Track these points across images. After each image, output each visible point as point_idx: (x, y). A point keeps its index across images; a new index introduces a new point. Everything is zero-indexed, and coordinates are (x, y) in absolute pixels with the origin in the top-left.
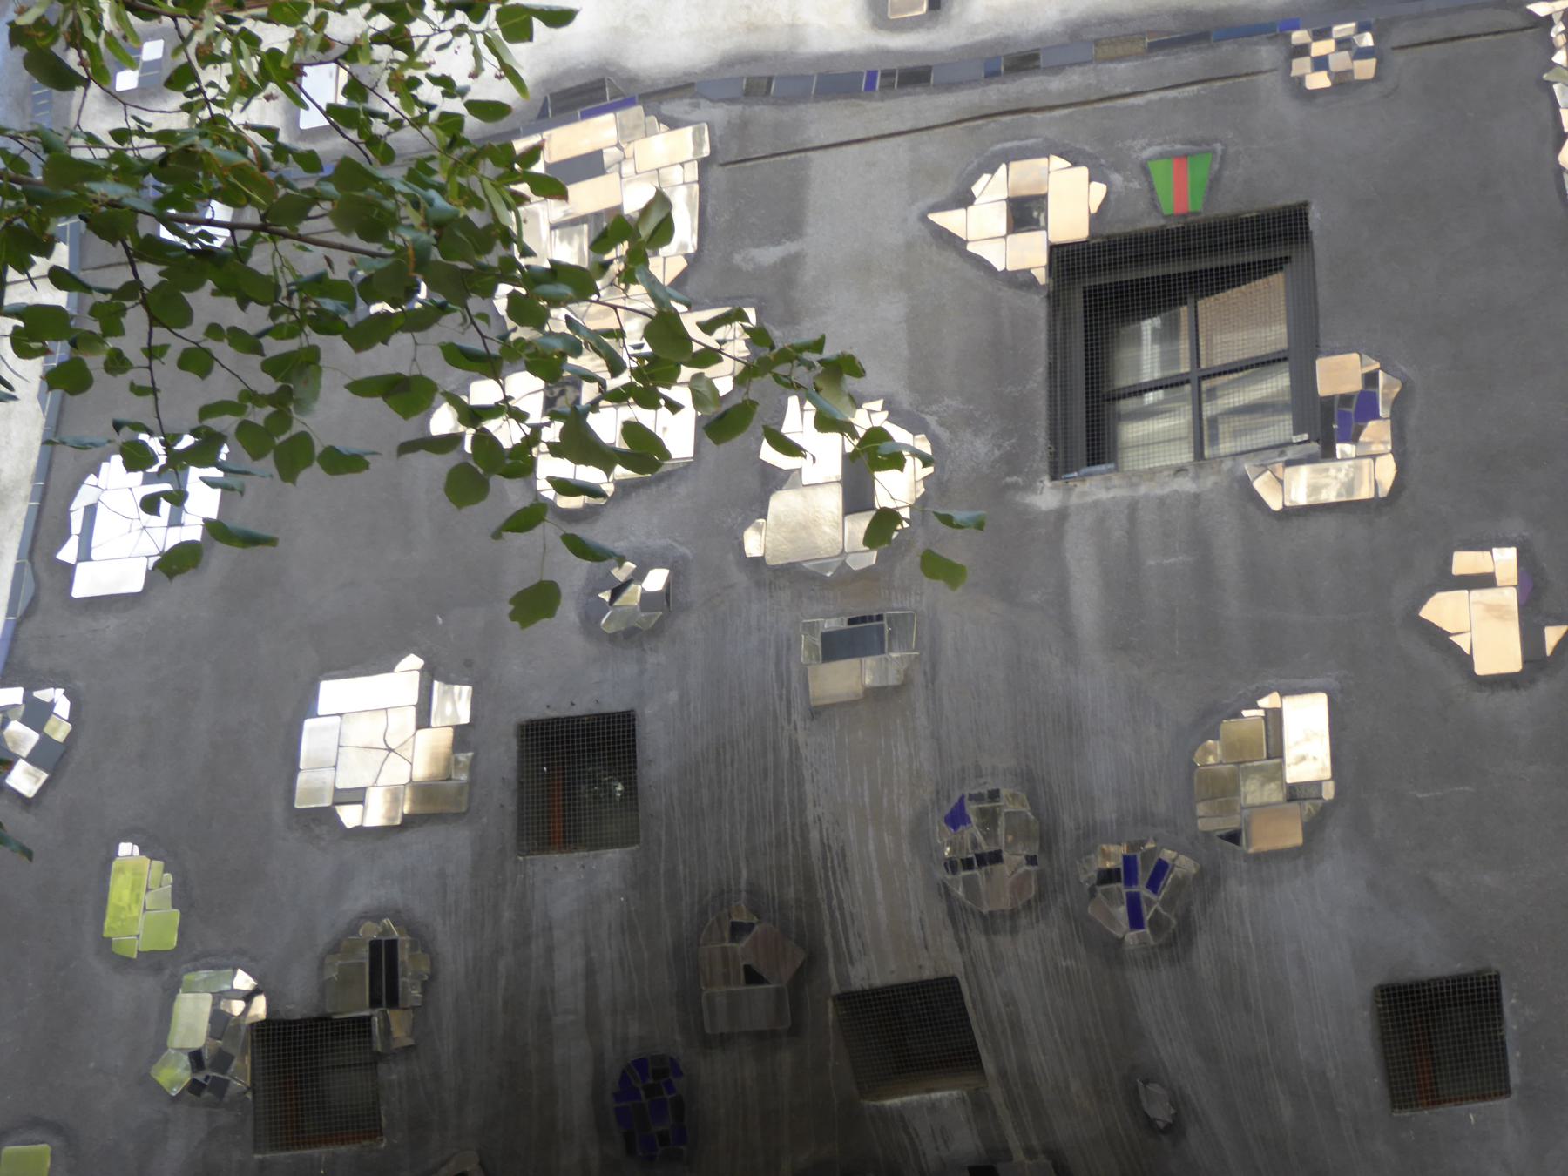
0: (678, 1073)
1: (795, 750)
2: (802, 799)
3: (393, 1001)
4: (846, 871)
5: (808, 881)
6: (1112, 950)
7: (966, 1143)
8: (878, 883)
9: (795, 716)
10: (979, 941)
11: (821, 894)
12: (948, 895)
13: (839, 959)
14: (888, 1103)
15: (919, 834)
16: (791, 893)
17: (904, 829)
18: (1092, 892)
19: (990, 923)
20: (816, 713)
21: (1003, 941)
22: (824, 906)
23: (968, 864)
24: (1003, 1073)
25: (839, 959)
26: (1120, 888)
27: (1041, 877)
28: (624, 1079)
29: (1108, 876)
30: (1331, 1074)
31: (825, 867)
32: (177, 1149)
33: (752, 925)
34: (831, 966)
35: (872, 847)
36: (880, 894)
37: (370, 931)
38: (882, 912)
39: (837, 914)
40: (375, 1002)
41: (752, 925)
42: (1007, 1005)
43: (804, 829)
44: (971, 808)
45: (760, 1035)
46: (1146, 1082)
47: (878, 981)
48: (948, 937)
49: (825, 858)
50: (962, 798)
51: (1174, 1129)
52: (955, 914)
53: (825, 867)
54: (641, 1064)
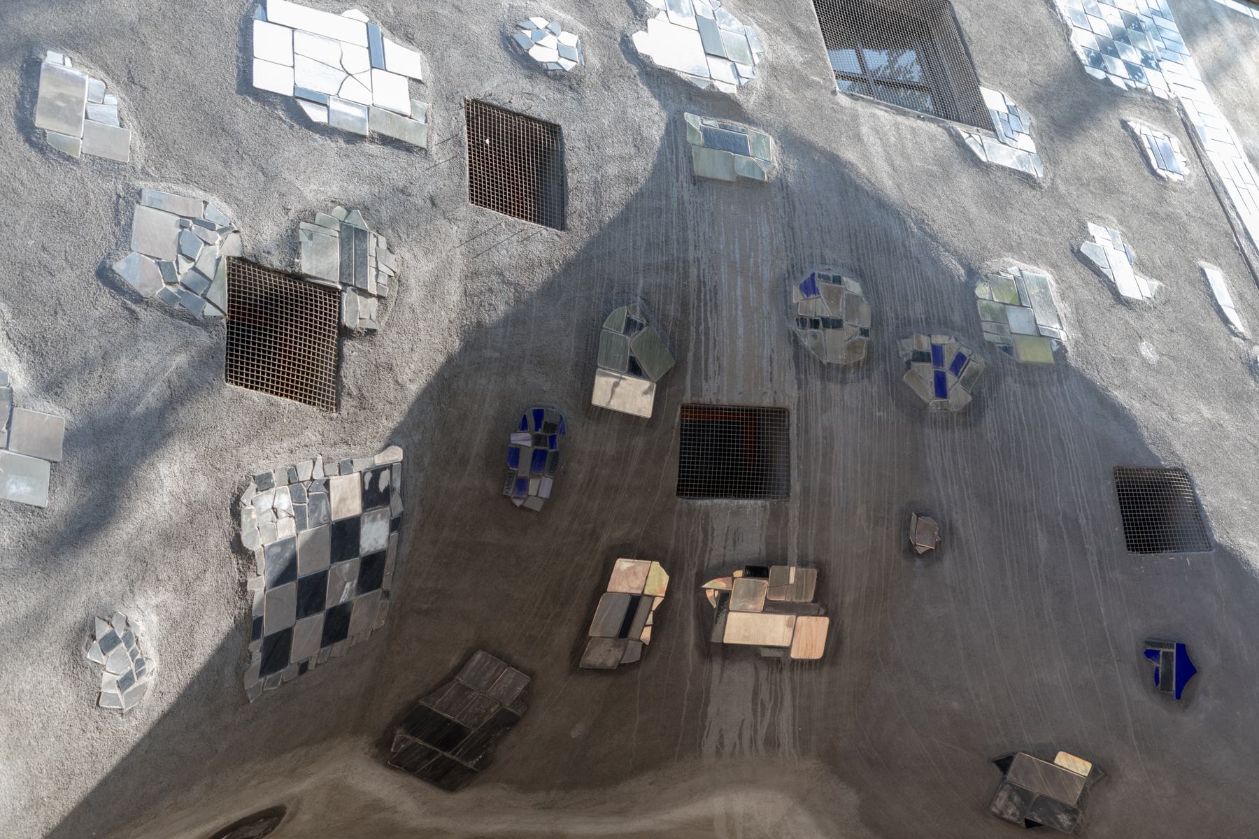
0: (563, 432)
1: (681, 202)
2: (685, 240)
4: (716, 306)
6: (917, 411)
8: (741, 321)
9: (681, 177)
10: (815, 384)
11: (692, 318)
12: (796, 342)
13: (696, 372)
15: (780, 293)
17: (766, 285)
18: (908, 364)
19: (826, 371)
21: (834, 388)
22: (693, 329)
23: (815, 324)
24: (806, 491)
25: (696, 372)
27: (869, 346)
29: (921, 357)
30: (1083, 521)
31: (699, 300)
33: (641, 326)
34: (688, 377)
35: (739, 293)
36: (741, 330)
38: (740, 344)
39: (703, 338)
42: (825, 438)
44: (820, 284)
47: (725, 400)
48: (790, 375)
49: (699, 291)
50: (813, 275)
52: (800, 358)
53: (699, 300)
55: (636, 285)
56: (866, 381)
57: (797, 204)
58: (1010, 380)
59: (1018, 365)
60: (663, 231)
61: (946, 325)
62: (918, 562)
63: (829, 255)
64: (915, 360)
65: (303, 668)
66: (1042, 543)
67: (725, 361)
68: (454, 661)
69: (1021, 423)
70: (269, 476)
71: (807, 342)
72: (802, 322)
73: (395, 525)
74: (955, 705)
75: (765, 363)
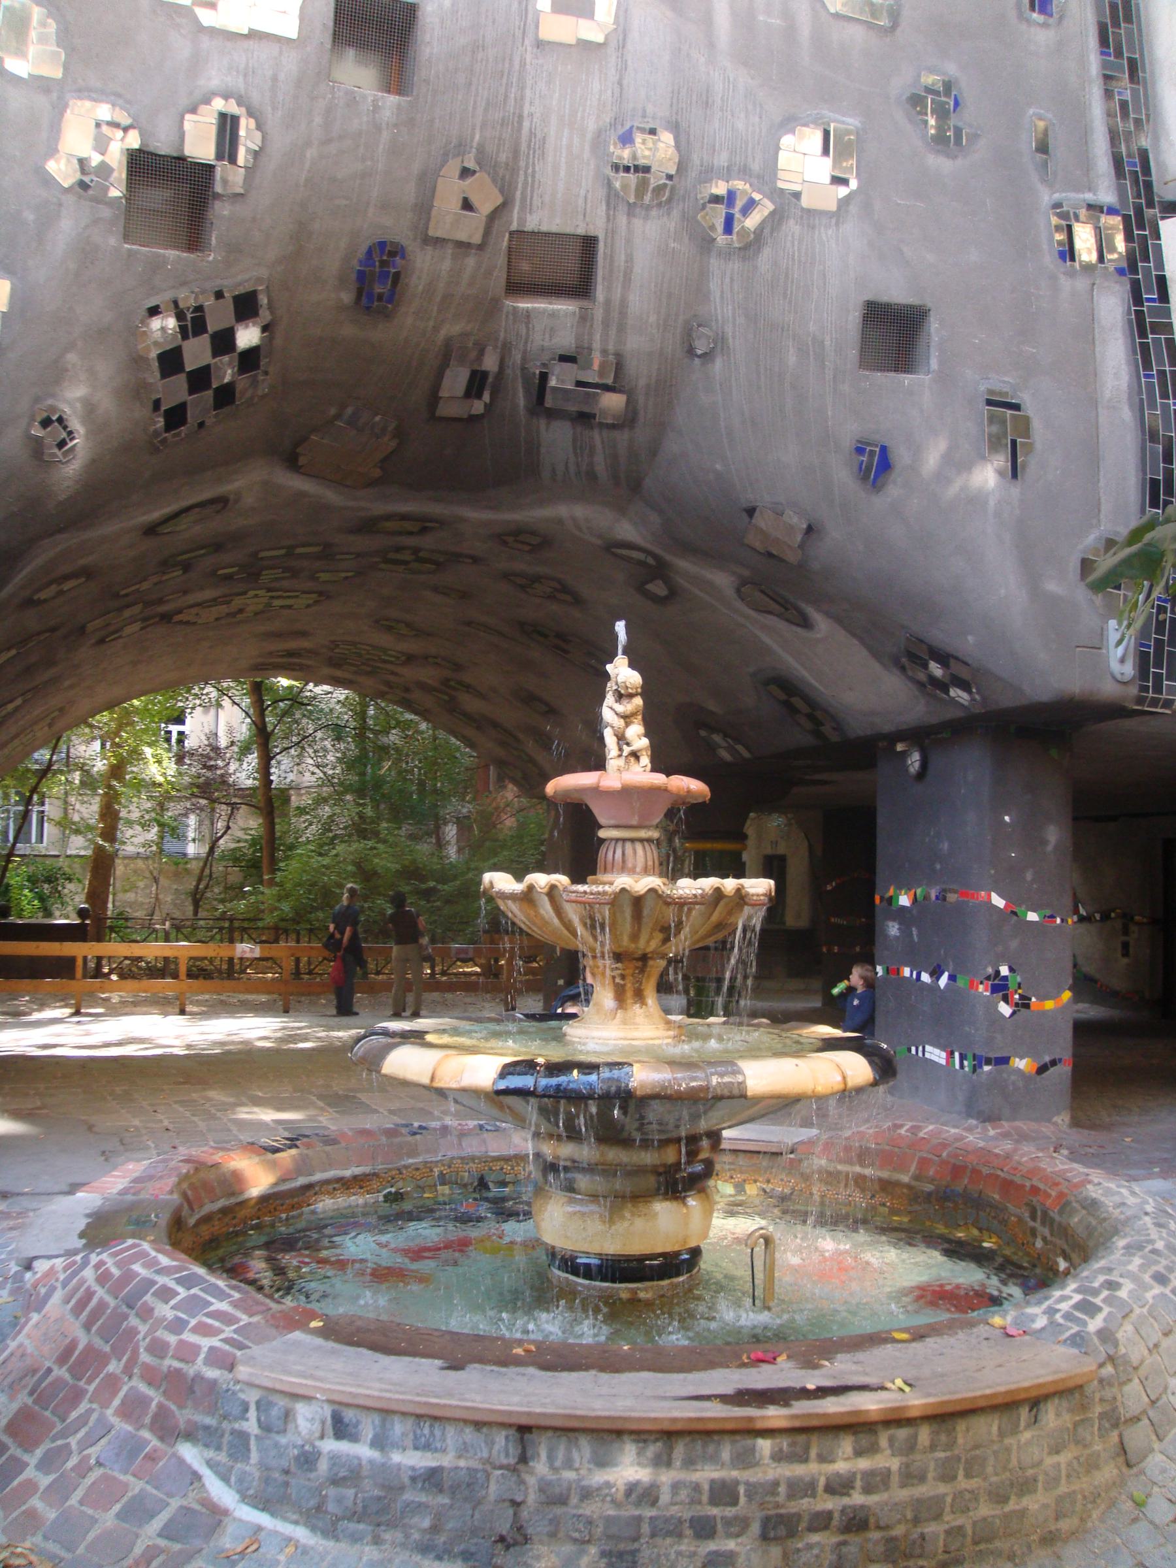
0: (403, 257)
1: (523, 64)
2: (522, 98)
3: (233, 160)
4: (543, 153)
5: (516, 153)
6: (706, 243)
7: (565, 340)
8: (563, 166)
9: (527, 42)
10: (622, 219)
11: (522, 164)
12: (609, 184)
14: (521, 305)
16: (503, 157)
17: (589, 136)
18: (704, 207)
20: (540, 44)
21: (637, 223)
22: (522, 172)
23: (627, 169)
24: (608, 303)
25: (523, 208)
26: (721, 209)
28: (369, 252)
29: (716, 199)
30: (827, 343)
31: (529, 146)
32: (68, 227)
33: (474, 172)
36: (562, 174)
37: (219, 104)
38: (561, 186)
39: (530, 179)
40: (219, 156)
41: (474, 172)
42: (627, 262)
43: (521, 117)
45: (460, 245)
46: (699, 326)
47: (544, 228)
48: (602, 210)
49: (530, 141)
50: (632, 127)
51: (707, 356)
52: (612, 198)
54: (382, 245)
55: (472, 141)
56: (665, 218)
57: (629, 63)
58: (792, 222)
59: (803, 209)
60: (502, 90)
61: (744, 172)
62: (697, 361)
63: (650, 109)
64: (710, 202)
65: (201, 425)
66: (792, 359)
67: (547, 199)
68: (333, 411)
69: (793, 259)
70: (158, 306)
71: (617, 185)
72: (616, 167)
73: (265, 329)
74: (718, 467)
75: (581, 201)
